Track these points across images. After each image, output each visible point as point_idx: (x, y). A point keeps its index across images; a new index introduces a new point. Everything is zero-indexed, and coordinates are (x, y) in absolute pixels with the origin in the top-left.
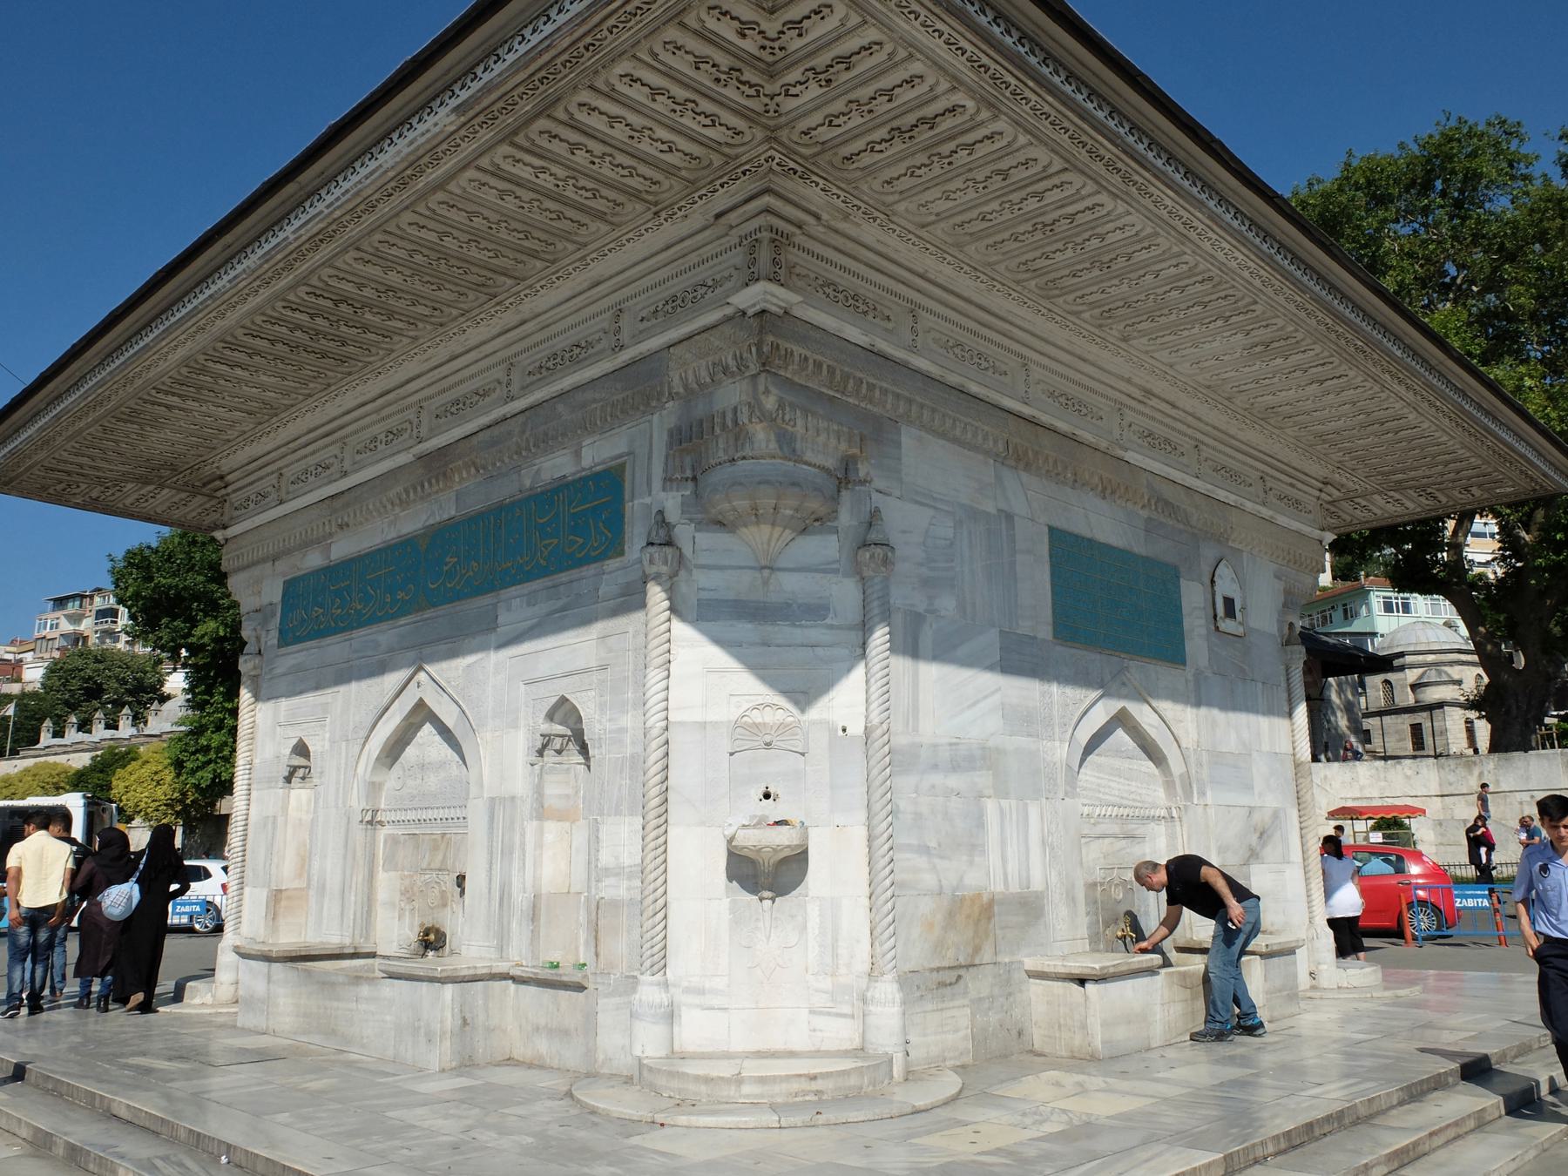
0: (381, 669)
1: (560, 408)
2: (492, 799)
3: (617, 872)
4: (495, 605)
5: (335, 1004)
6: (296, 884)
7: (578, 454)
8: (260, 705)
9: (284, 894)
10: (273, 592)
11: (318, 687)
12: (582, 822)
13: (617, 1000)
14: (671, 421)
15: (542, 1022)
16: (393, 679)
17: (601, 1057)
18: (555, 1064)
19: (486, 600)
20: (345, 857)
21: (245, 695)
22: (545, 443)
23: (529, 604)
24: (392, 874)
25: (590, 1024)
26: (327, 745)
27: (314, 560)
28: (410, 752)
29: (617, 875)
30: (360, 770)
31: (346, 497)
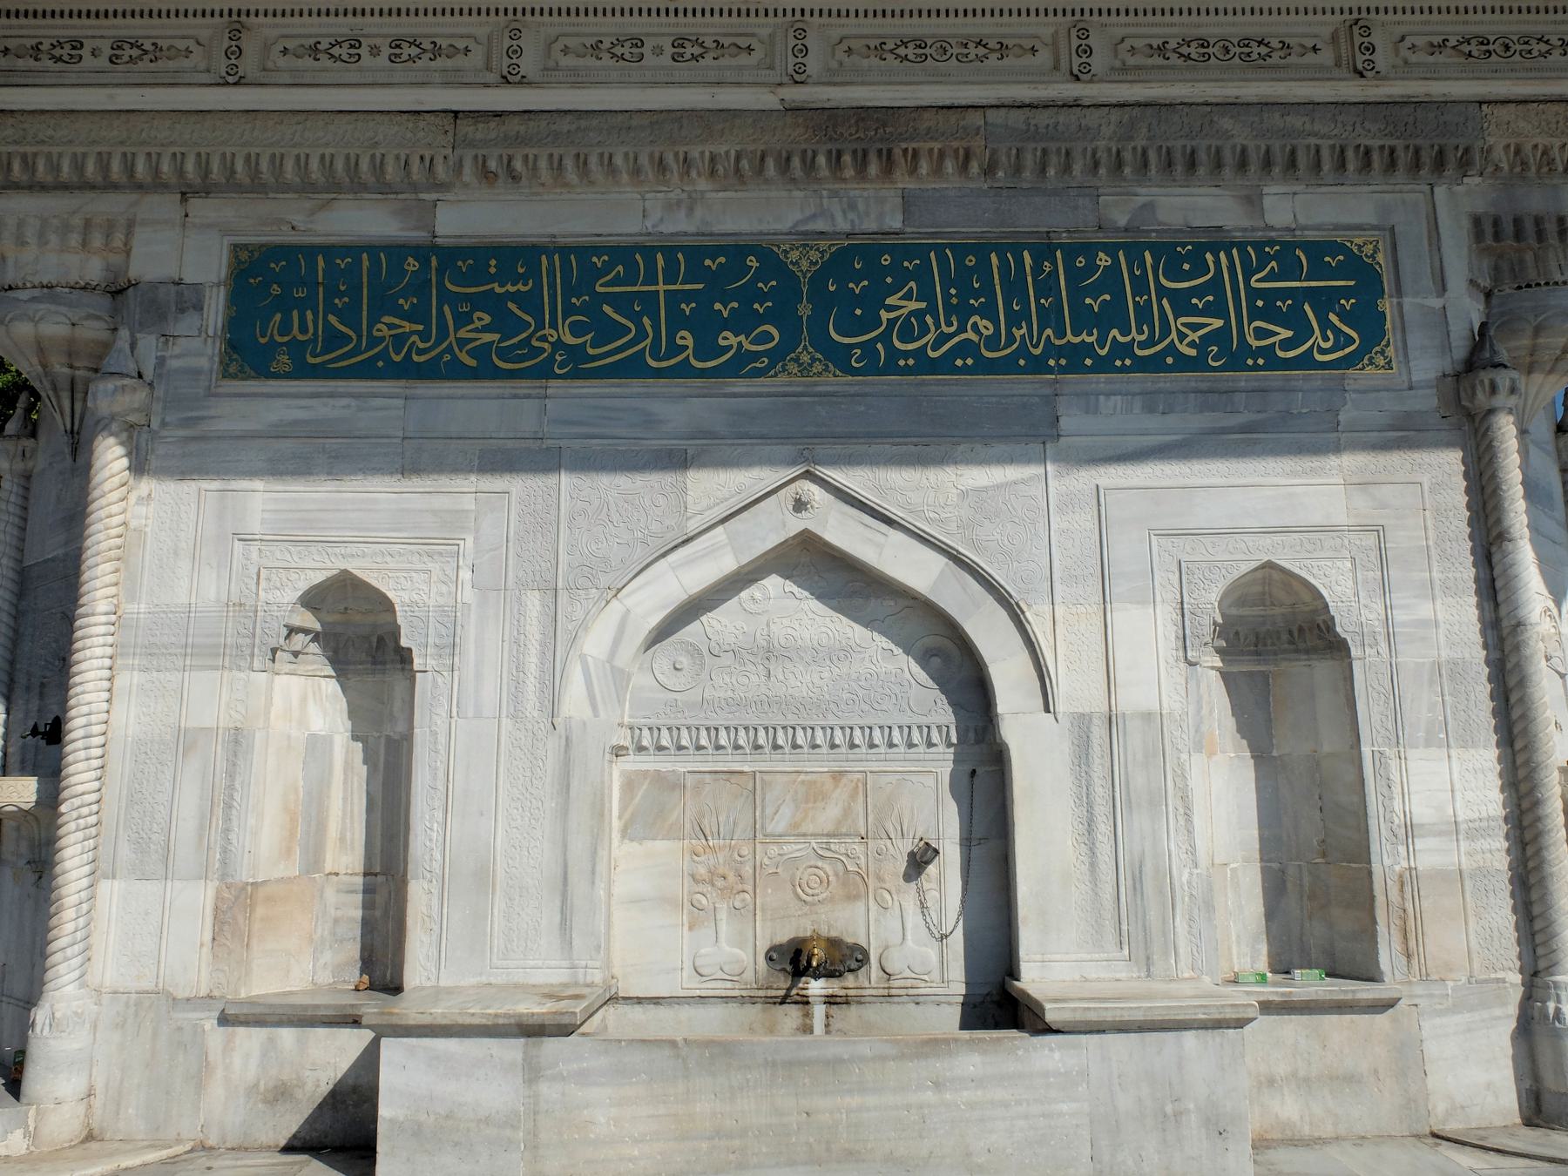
0: (677, 460)
1: (1226, 123)
2: (1082, 722)
3: (1455, 828)
4: (1050, 400)
5: (854, 1101)
6: (281, 871)
7: (1253, 201)
8: (146, 485)
9: (262, 892)
10: (189, 252)
11: (410, 467)
12: (1219, 757)
13: (1467, 1016)
14: (1480, 207)
15: (1281, 1069)
16: (711, 488)
17: (1441, 1107)
18: (1327, 1130)
19: (1025, 386)
20: (564, 812)
21: (111, 457)
22: (1186, 165)
23: (1150, 409)
24: (660, 845)
25: (1409, 1060)
26: (468, 595)
27: (367, 221)
28: (721, 623)
29: (1440, 834)
30: (595, 643)
31: (514, 126)
